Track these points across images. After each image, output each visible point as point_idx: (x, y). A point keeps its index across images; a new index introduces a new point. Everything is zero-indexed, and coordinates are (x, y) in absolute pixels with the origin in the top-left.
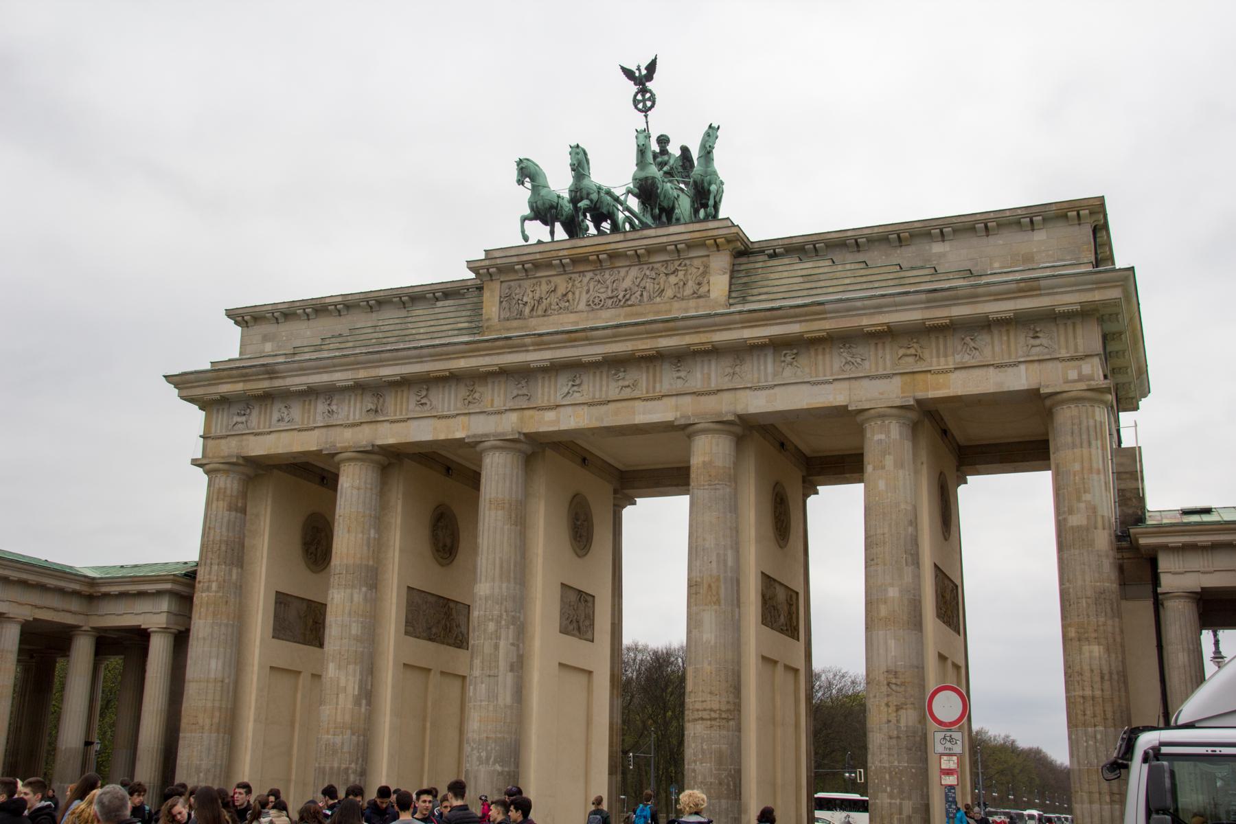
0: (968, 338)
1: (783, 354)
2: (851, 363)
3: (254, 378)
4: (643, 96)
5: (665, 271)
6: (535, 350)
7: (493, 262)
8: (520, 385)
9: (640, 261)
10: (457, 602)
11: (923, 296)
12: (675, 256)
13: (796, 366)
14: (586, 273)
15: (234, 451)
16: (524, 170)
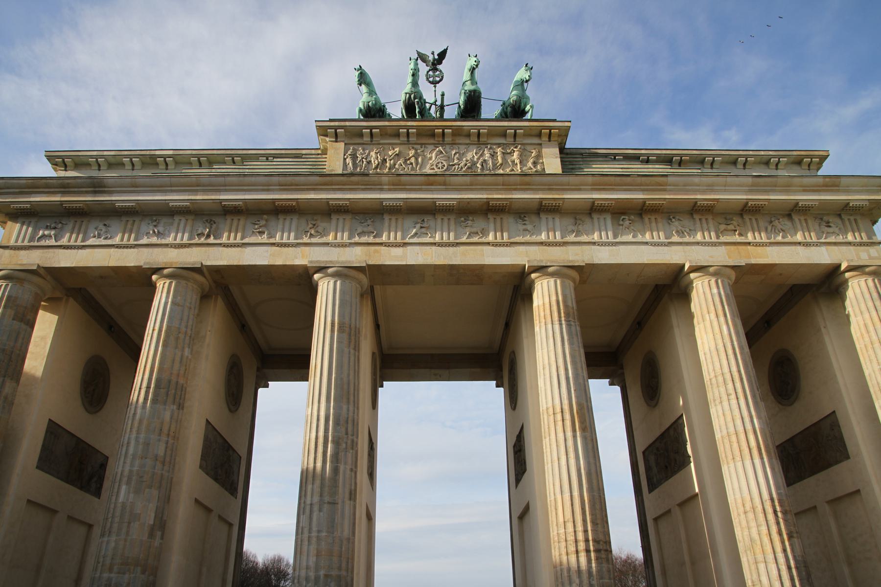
0: (776, 223)
1: (621, 219)
2: (681, 232)
3: (76, 190)
4: (434, 72)
5: (503, 151)
6: (390, 190)
7: (342, 124)
8: (366, 224)
9: (479, 141)
10: (234, 450)
11: (750, 180)
12: (510, 140)
13: (633, 230)
14: (427, 146)
15: (37, 261)
16: (362, 75)
